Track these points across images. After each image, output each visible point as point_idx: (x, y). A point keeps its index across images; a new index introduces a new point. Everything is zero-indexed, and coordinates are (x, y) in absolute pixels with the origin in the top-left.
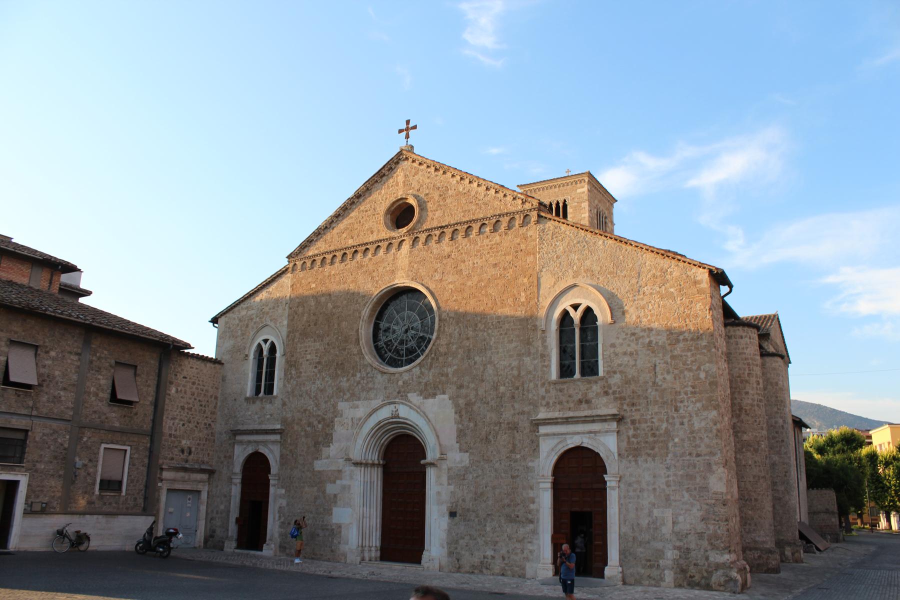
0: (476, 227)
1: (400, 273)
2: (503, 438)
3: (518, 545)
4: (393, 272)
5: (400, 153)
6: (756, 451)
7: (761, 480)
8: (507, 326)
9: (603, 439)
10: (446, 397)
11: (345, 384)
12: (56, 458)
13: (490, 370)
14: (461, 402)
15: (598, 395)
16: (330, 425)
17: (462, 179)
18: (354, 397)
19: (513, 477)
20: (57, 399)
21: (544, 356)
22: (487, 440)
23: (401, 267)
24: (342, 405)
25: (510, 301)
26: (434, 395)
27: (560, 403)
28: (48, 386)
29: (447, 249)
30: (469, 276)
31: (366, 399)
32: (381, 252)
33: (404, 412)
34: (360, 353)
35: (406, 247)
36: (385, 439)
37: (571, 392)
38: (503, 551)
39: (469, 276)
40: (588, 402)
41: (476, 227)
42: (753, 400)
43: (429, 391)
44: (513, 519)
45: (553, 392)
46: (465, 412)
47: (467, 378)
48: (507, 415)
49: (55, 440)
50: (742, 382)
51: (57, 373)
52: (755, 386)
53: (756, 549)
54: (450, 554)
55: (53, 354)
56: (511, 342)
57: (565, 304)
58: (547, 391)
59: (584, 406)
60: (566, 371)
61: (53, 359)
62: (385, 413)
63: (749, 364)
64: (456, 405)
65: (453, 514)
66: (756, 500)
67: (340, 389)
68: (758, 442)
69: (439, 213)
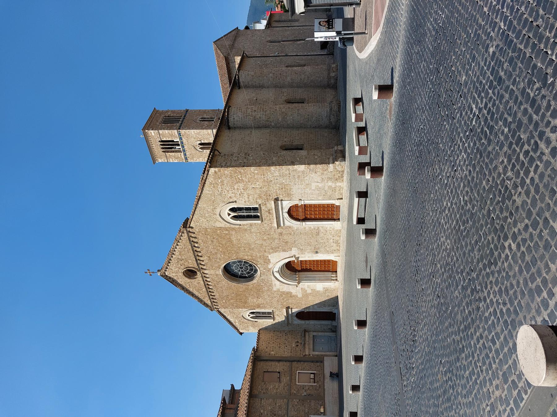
0: (195, 249)
1: (217, 273)
2: (285, 237)
3: (328, 232)
4: (217, 275)
5: (162, 276)
6: (286, 114)
7: (300, 112)
8: (239, 237)
9: (284, 206)
10: (269, 256)
11: (266, 288)
12: (303, 404)
13: (257, 242)
14: (271, 251)
15: (266, 207)
16: (283, 293)
17: (173, 254)
18: (271, 285)
19: (301, 234)
20: (280, 407)
21: (251, 225)
22: (287, 242)
23: (215, 272)
24: (275, 289)
25: (228, 237)
26: (269, 260)
27: (270, 219)
28: (275, 412)
29: (206, 257)
30: (217, 250)
31: (272, 281)
32: (208, 280)
33: (276, 269)
34: (253, 284)
35: (205, 272)
36: (289, 272)
37: (266, 215)
38: (331, 236)
39: (217, 250)
40: (269, 210)
41: (195, 249)
42: (263, 114)
43: (267, 261)
44: (318, 234)
45: (266, 222)
46: (275, 250)
47: (261, 249)
48: (276, 236)
49: (296, 405)
50: (255, 120)
51: (270, 408)
52: (256, 113)
53: (330, 116)
54: (332, 253)
55: (262, 411)
56: (245, 236)
57: (228, 218)
58: (266, 224)
59: (271, 211)
60: (256, 217)
61: (264, 410)
62: (277, 275)
63: (246, 116)
64: (273, 252)
65: (317, 252)
66: (308, 115)
67: (268, 290)
68: (282, 113)
69: (190, 261)
